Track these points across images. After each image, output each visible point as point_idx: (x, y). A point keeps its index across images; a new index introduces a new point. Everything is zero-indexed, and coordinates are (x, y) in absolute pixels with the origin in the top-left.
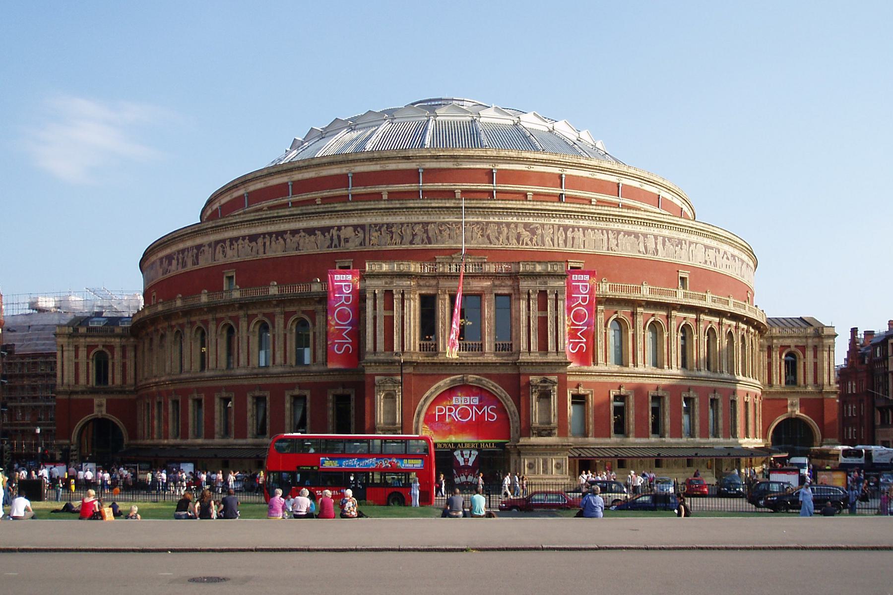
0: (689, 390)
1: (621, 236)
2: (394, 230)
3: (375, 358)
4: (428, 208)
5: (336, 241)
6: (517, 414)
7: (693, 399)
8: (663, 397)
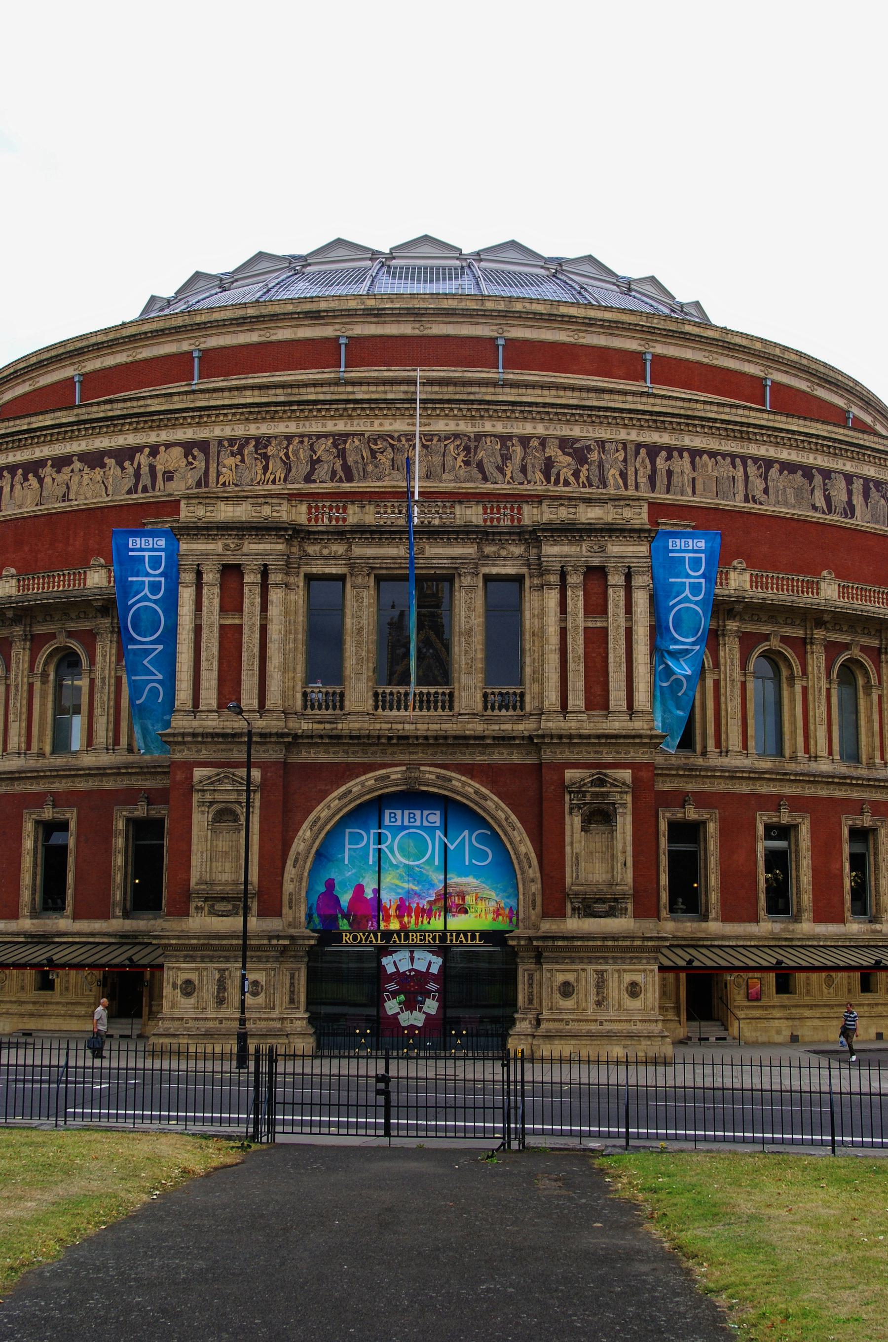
1: (774, 472)
2: (270, 451)
3: (196, 723)
4: (348, 401)
5: (146, 480)
6: (535, 862)
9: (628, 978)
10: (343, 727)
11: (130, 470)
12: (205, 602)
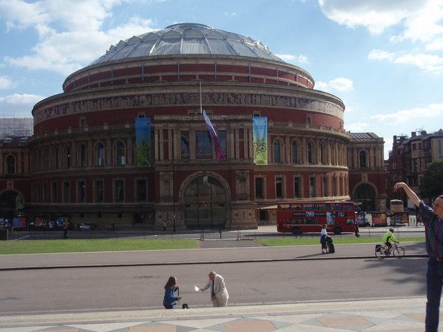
8: (300, 178)
11: (133, 100)
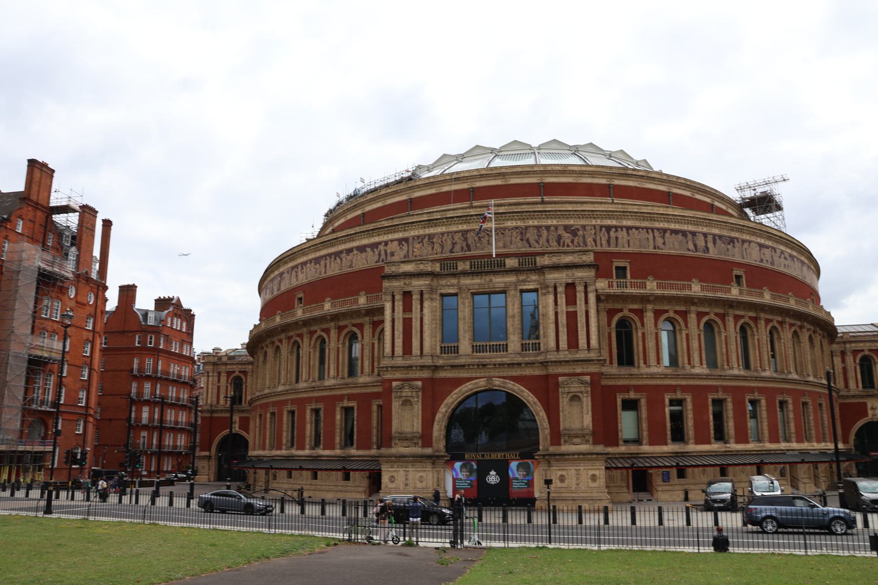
0: (753, 392)
1: (668, 235)
2: (435, 240)
3: (393, 362)
5: (383, 256)
6: (546, 420)
7: (759, 401)
8: (725, 400)
9: (591, 473)
10: (457, 362)
12: (396, 308)
